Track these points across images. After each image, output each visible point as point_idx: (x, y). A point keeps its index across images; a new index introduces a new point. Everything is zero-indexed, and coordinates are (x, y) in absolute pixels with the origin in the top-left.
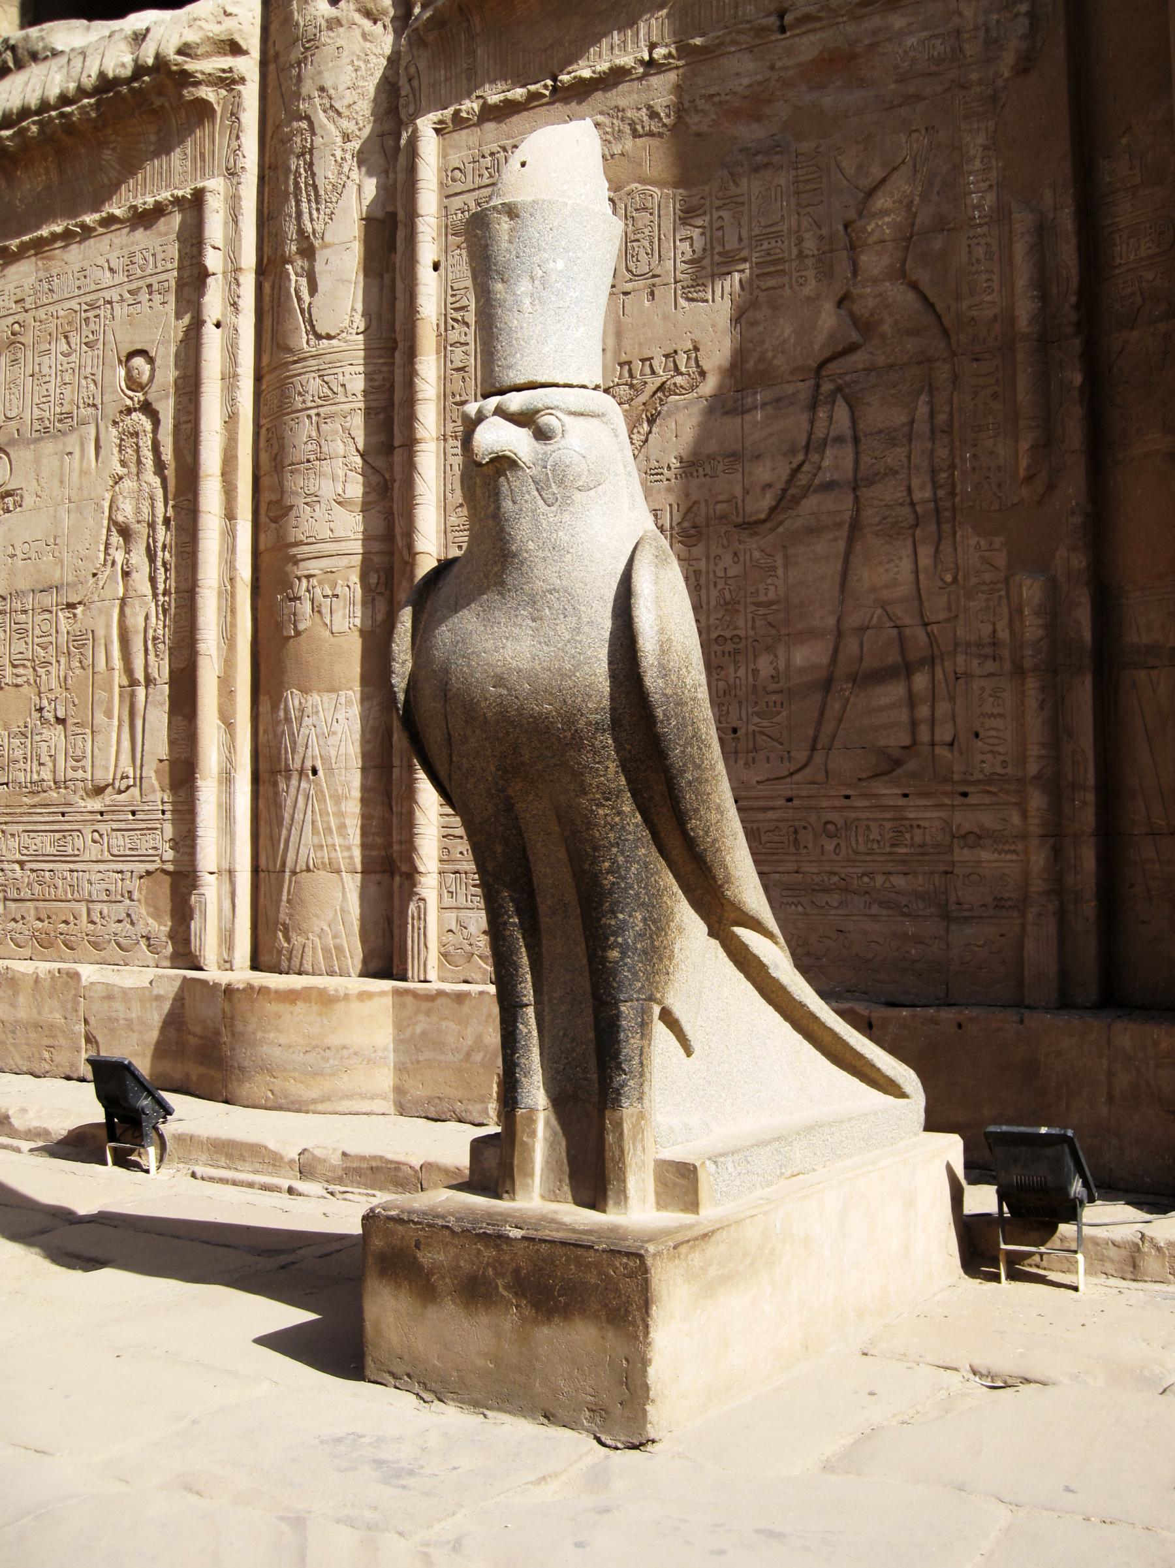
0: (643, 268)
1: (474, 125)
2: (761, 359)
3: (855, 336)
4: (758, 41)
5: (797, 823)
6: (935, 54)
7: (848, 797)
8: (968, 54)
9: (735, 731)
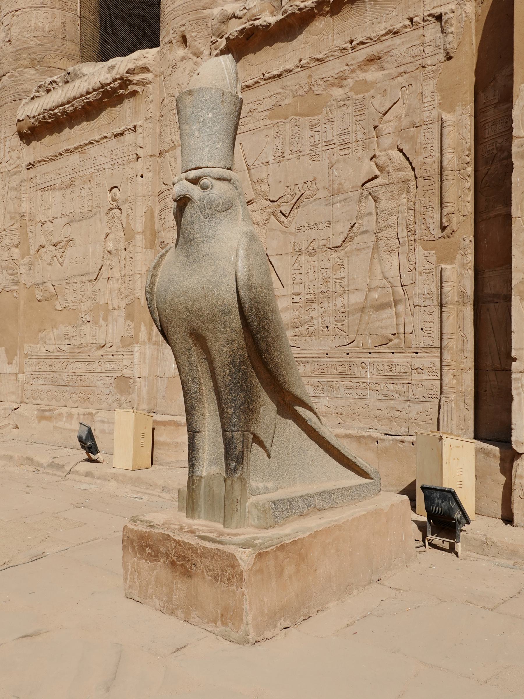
0: (296, 149)
2: (340, 184)
3: (378, 173)
4: (341, 54)
5: (350, 363)
7: (370, 353)
9: (327, 327)
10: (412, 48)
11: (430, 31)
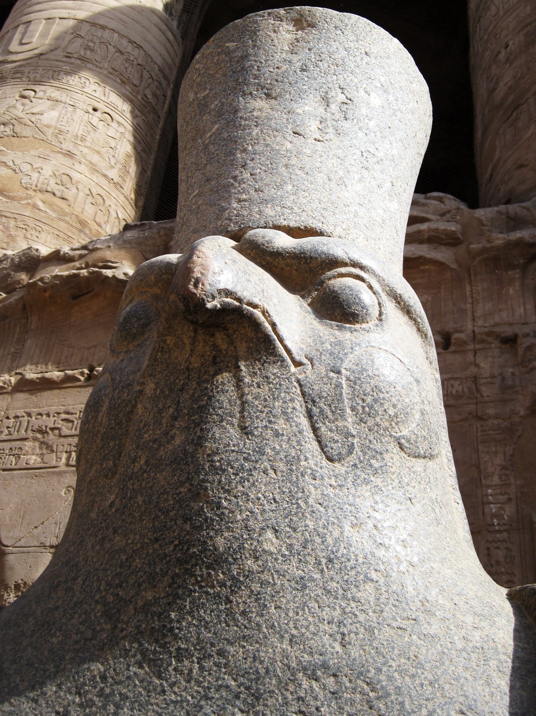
1: (7, 393)
6: (454, 392)
8: (485, 395)
10: (452, 382)
11: (490, 359)
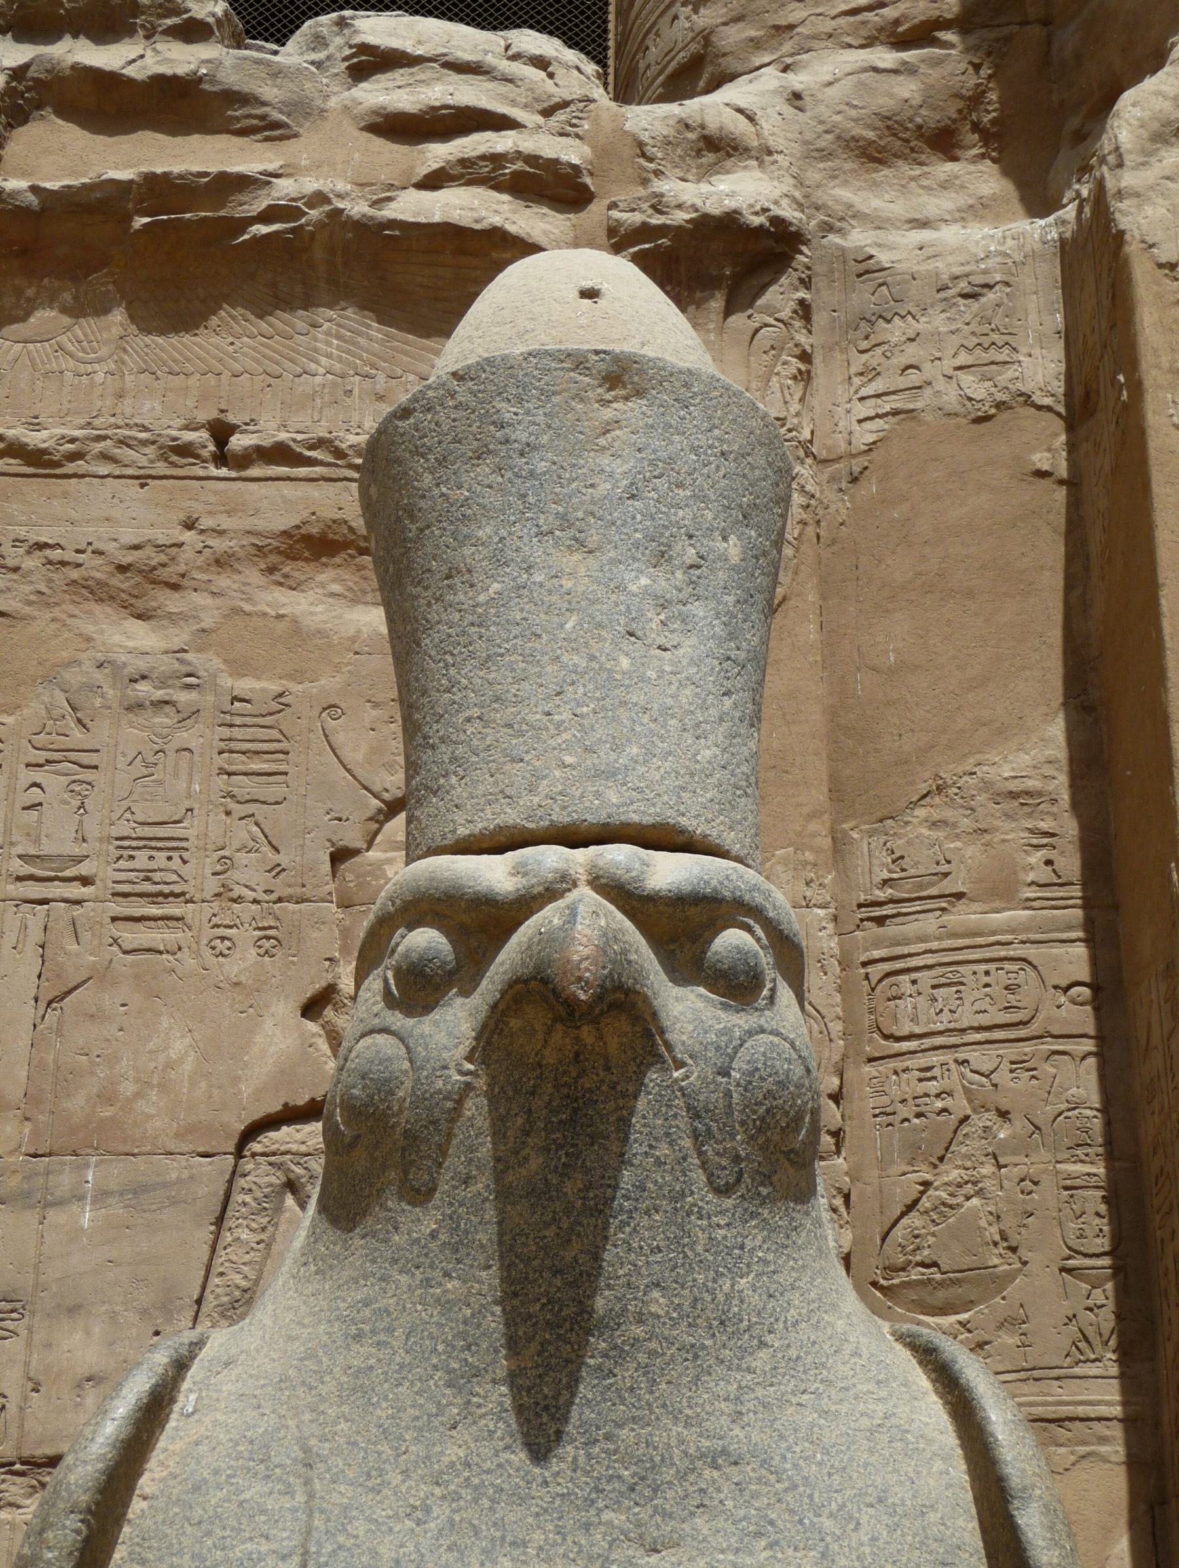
2: (107, 1096)
4: (161, 468)
